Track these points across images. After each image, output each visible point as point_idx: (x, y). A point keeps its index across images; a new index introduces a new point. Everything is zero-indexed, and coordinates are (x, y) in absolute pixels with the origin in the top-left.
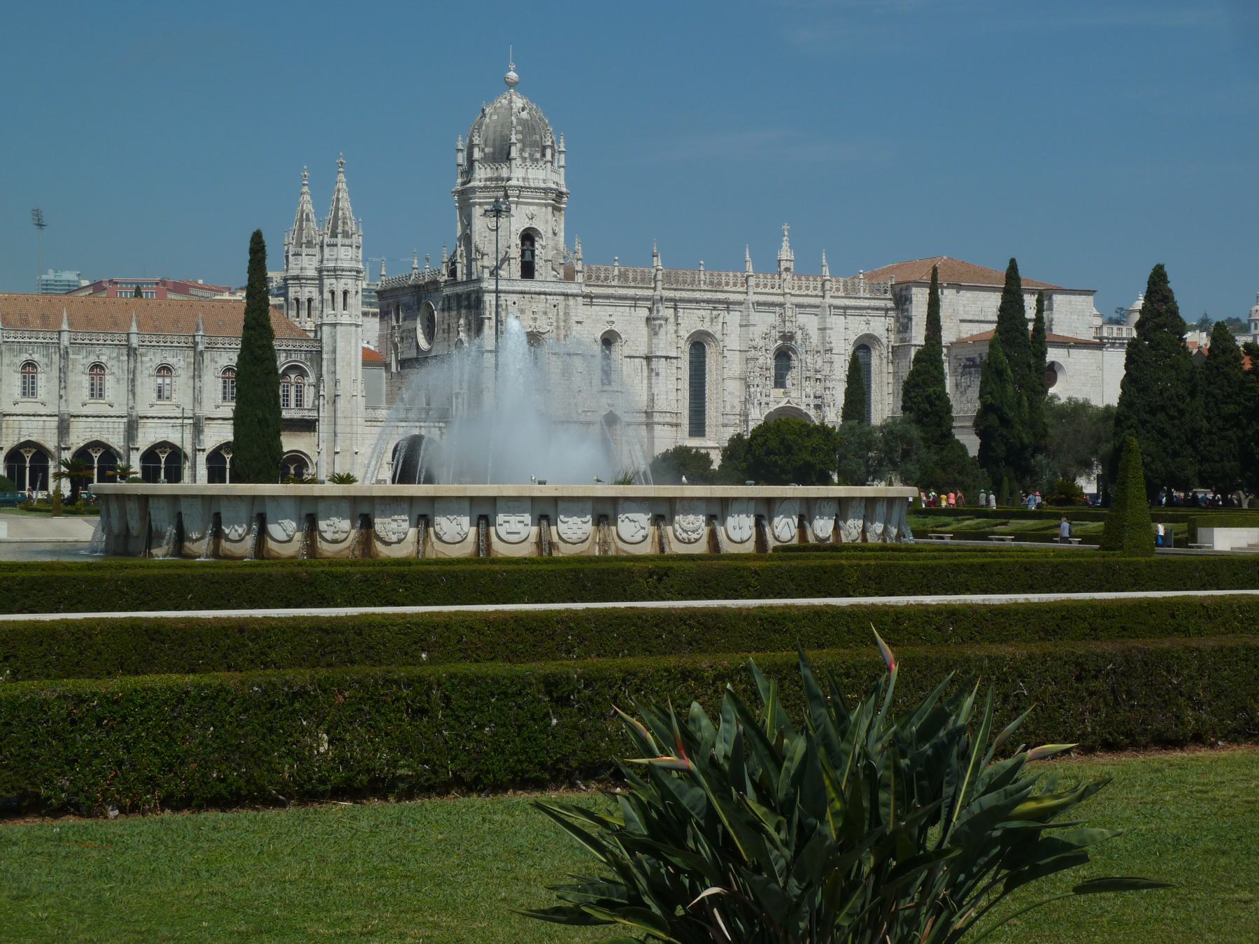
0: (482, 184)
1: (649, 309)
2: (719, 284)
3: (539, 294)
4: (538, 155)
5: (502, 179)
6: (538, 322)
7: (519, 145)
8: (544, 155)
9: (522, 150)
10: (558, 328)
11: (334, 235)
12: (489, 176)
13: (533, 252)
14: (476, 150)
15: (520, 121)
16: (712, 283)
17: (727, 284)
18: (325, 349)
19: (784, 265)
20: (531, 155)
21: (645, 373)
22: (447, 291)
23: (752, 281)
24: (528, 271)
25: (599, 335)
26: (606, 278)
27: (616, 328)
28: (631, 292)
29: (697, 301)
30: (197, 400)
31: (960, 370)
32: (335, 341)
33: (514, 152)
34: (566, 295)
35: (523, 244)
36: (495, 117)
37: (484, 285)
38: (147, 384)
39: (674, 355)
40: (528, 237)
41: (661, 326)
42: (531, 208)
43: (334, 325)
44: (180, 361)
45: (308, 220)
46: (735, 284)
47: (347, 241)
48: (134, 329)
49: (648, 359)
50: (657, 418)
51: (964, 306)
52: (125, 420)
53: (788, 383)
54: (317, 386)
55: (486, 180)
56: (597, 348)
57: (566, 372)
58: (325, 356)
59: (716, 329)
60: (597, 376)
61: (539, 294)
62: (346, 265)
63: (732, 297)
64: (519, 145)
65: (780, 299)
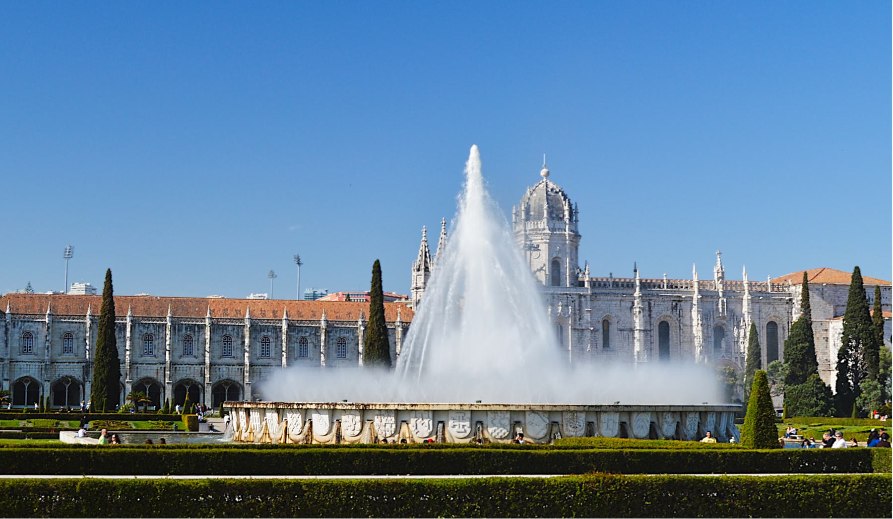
0: (528, 232)
3: (564, 294)
5: (540, 230)
8: (564, 216)
10: (575, 314)
12: (532, 227)
17: (682, 287)
20: (557, 216)
26: (605, 285)
27: (613, 315)
28: (621, 292)
31: (836, 336)
34: (580, 296)
35: (553, 267)
36: (535, 195)
39: (648, 328)
46: (687, 288)
51: (839, 297)
53: (723, 345)
55: (530, 230)
56: (600, 326)
60: (600, 342)
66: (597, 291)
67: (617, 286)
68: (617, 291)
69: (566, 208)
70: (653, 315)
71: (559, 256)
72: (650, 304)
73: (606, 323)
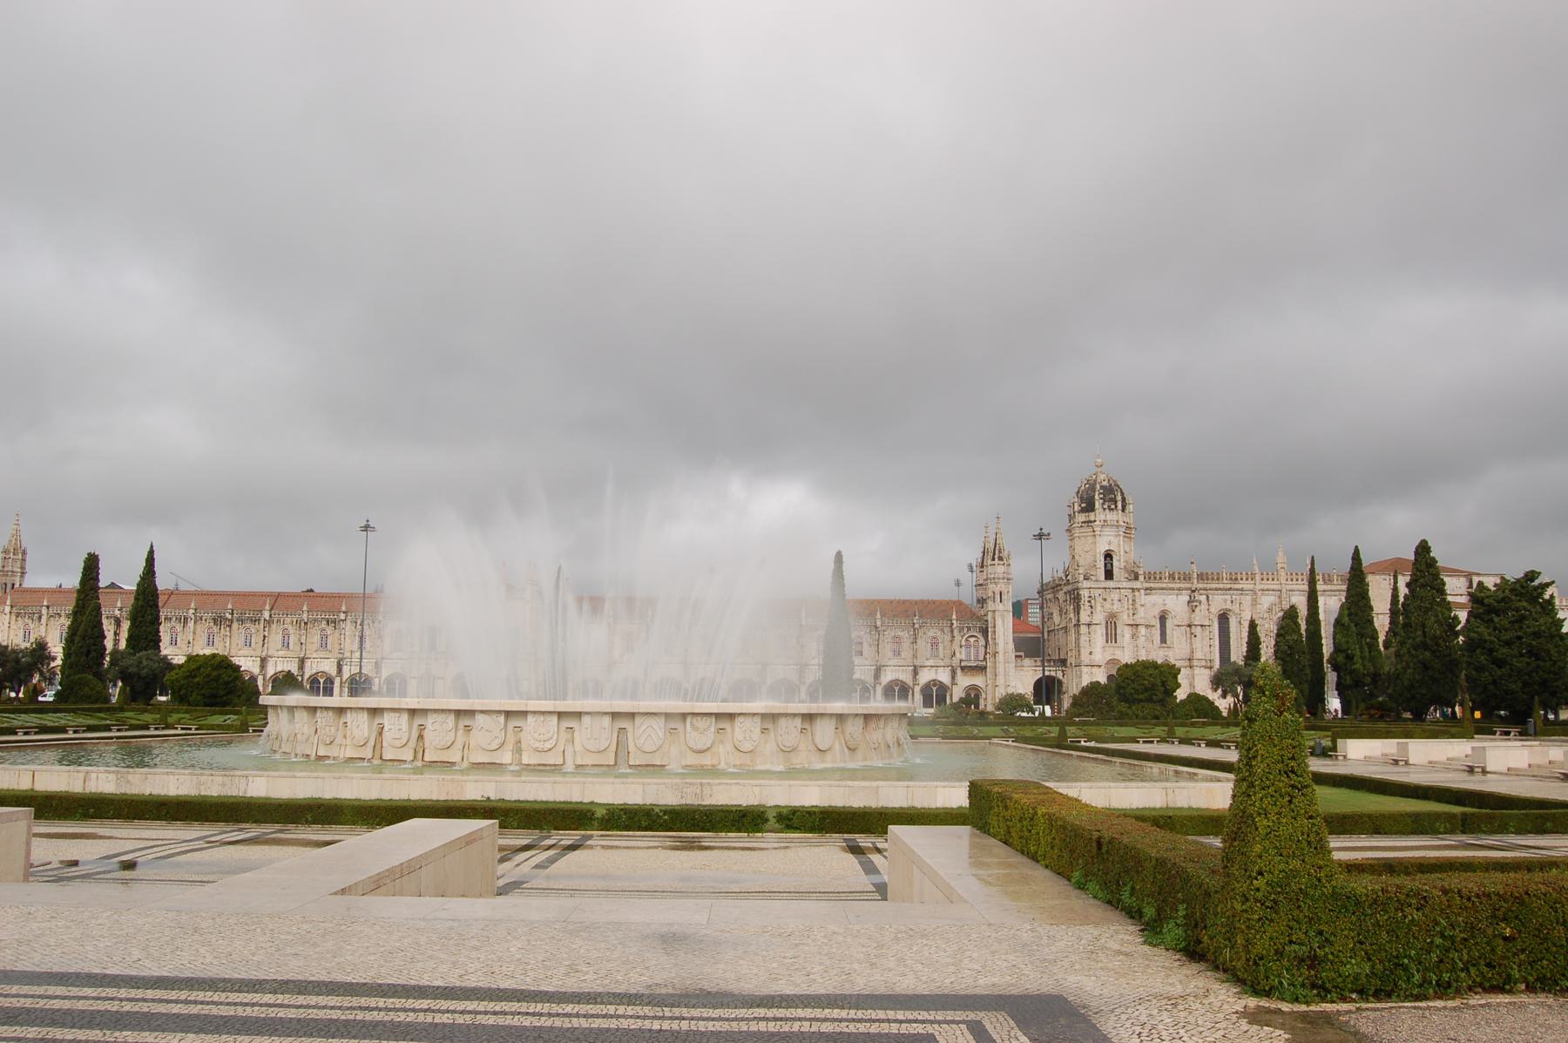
1: (1190, 597)
2: (1236, 579)
3: (1116, 588)
4: (1113, 507)
5: (1091, 522)
6: (1115, 607)
7: (1101, 501)
8: (1116, 507)
9: (1103, 504)
10: (1128, 609)
11: (993, 559)
12: (1084, 520)
13: (1112, 565)
14: (1076, 505)
15: (1102, 487)
16: (1231, 579)
17: (1242, 579)
18: (990, 625)
19: (1279, 566)
20: (1109, 507)
21: (1188, 635)
22: (1065, 589)
23: (1258, 577)
24: (1109, 575)
25: (1157, 612)
26: (1161, 578)
27: (1167, 608)
28: (1178, 586)
29: (1220, 589)
30: (915, 656)
32: (995, 621)
33: (1097, 506)
34: (1133, 590)
35: (1105, 560)
37: (1080, 585)
38: (887, 649)
40: (1108, 556)
41: (1196, 606)
42: (1110, 538)
43: (994, 611)
44: (905, 635)
45: (988, 552)
47: (1002, 563)
48: (878, 616)
49: (1189, 626)
50: (1195, 663)
52: (875, 667)
54: (986, 647)
55: (1082, 523)
57: (1134, 636)
58: (989, 629)
59: (1235, 608)
60: (1157, 637)
61: (1116, 588)
62: (1001, 576)
63: (1245, 587)
64: (1101, 501)
65: (1278, 587)
66: (1152, 585)
67: (1174, 579)
69: (1119, 498)
70: (1212, 610)
71: (1112, 548)
72: (1208, 597)
73: (1163, 619)
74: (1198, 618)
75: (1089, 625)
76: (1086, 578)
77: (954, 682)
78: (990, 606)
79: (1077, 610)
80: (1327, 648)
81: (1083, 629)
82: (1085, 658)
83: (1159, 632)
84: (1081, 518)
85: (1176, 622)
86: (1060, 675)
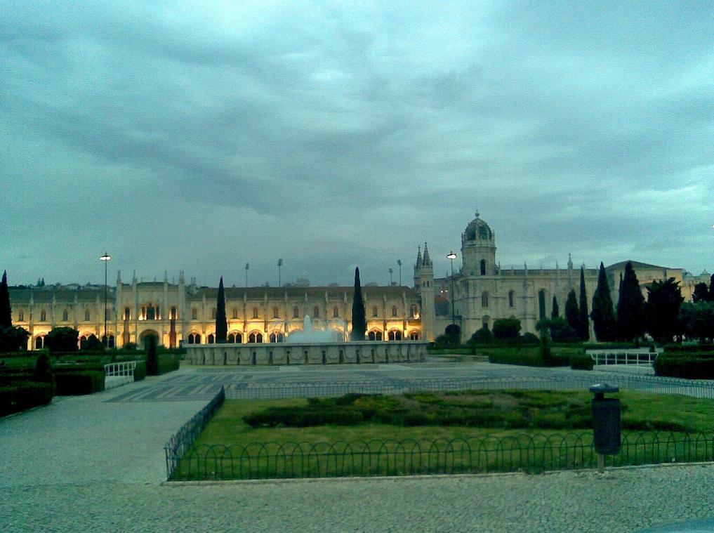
11: (424, 265)
15: (480, 227)
22: (461, 279)
24: (483, 272)
25: (507, 290)
27: (514, 289)
28: (518, 277)
33: (477, 237)
34: (496, 279)
40: (483, 263)
56: (508, 297)
57: (496, 304)
59: (547, 288)
66: (506, 277)
68: (515, 277)
69: (488, 232)
70: (535, 289)
73: (511, 294)
74: (529, 294)
75: (474, 298)
76: (472, 274)
77: (405, 329)
78: (422, 289)
79: (467, 291)
80: (590, 309)
81: (471, 300)
82: (472, 315)
83: (509, 301)
84: (469, 243)
85: (517, 295)
86: (458, 324)
